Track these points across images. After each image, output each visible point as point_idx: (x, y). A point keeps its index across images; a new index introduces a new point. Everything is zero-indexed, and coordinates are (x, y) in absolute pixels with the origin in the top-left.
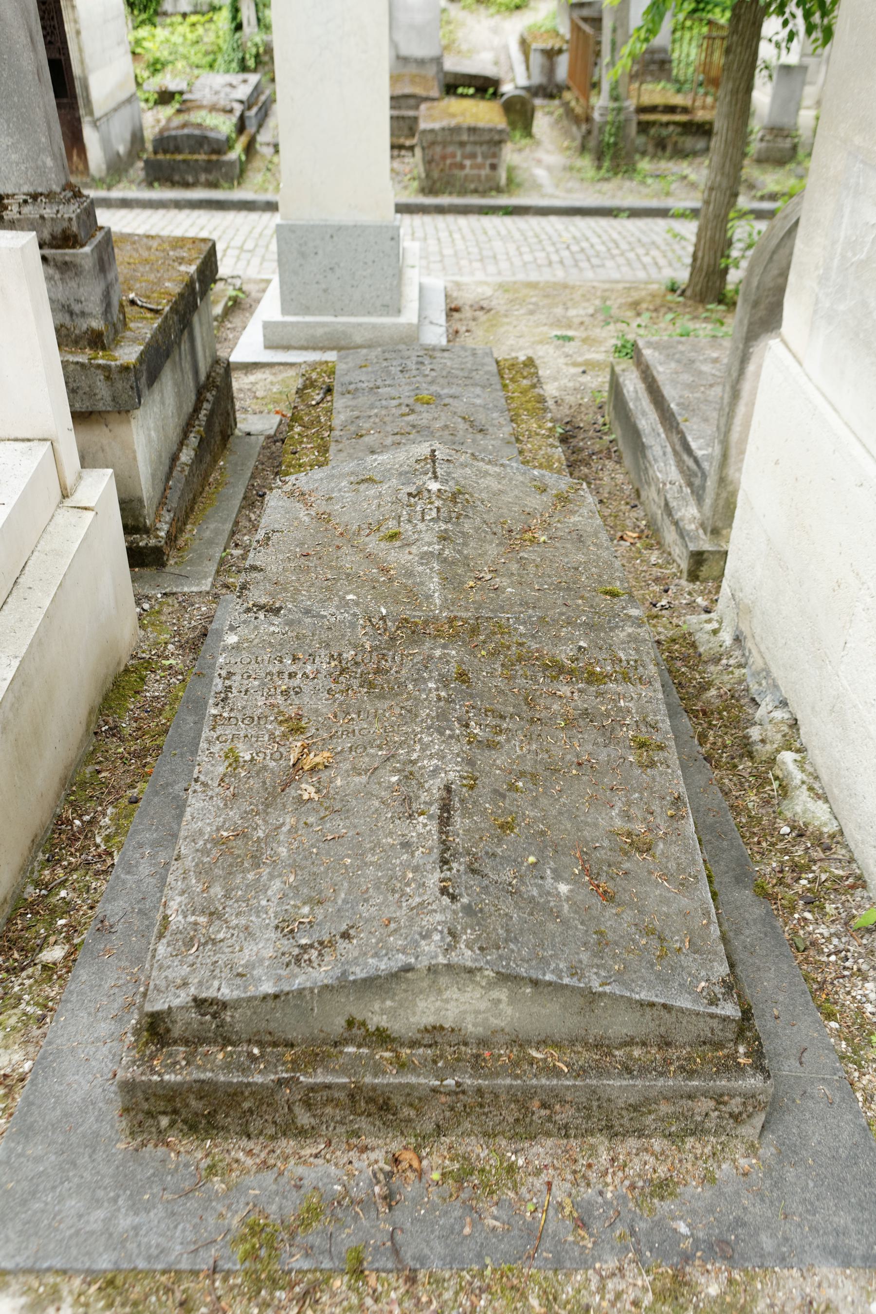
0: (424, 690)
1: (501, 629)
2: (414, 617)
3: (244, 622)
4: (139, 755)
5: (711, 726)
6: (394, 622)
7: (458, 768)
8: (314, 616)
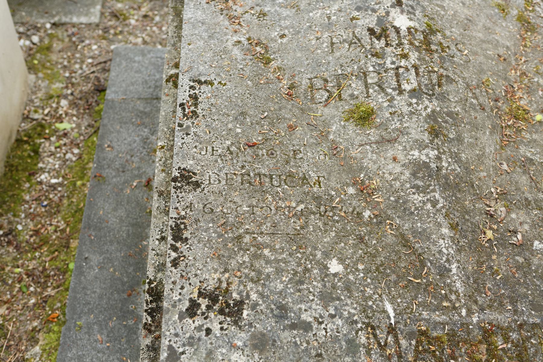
2: (436, 325)
3: (191, 342)
4: (39, 278)
6: (410, 336)
8: (293, 326)
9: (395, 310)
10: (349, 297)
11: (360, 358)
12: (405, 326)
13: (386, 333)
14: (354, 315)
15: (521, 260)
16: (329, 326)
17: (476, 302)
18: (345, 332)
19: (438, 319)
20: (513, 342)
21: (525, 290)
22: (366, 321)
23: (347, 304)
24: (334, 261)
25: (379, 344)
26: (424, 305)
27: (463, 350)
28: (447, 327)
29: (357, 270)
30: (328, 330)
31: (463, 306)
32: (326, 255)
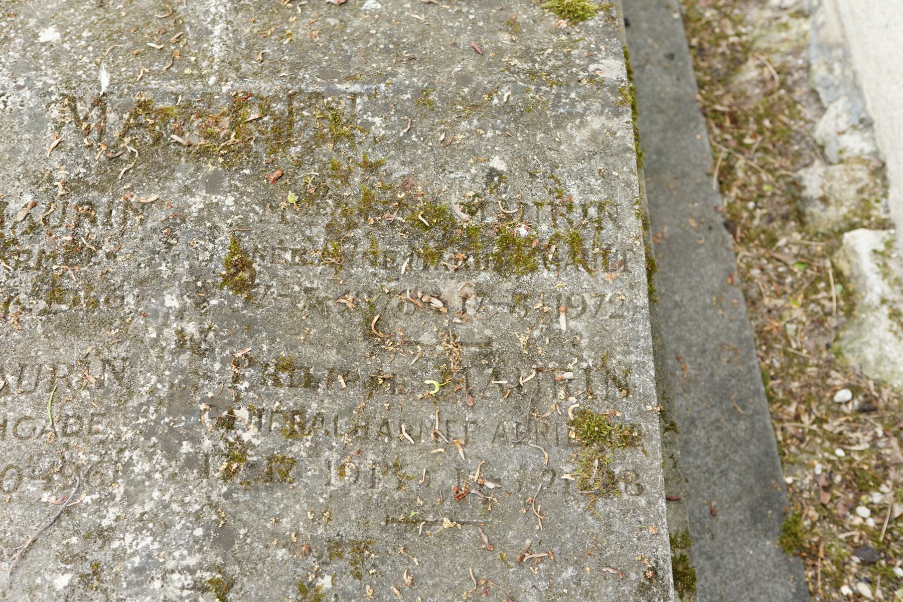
0: (155, 314)
1: (340, 127)
5: (741, 148)
6: (120, 110)
7: (192, 561)
9: (112, 79)
10: (53, 67)
11: (45, 135)
12: (121, 96)
13: (89, 106)
14: (50, 86)
15: (332, 21)
16: (10, 99)
17: (237, 70)
18: (32, 105)
19: (171, 89)
20: (273, 114)
21: (321, 56)
22: (66, 92)
23: (46, 75)
24: (52, 29)
25: (77, 118)
26: (156, 74)
27: (195, 124)
28: (180, 97)
29: (80, 38)
30: (9, 103)
31: (213, 74)
32: (42, 23)
